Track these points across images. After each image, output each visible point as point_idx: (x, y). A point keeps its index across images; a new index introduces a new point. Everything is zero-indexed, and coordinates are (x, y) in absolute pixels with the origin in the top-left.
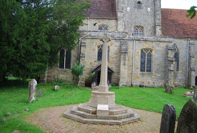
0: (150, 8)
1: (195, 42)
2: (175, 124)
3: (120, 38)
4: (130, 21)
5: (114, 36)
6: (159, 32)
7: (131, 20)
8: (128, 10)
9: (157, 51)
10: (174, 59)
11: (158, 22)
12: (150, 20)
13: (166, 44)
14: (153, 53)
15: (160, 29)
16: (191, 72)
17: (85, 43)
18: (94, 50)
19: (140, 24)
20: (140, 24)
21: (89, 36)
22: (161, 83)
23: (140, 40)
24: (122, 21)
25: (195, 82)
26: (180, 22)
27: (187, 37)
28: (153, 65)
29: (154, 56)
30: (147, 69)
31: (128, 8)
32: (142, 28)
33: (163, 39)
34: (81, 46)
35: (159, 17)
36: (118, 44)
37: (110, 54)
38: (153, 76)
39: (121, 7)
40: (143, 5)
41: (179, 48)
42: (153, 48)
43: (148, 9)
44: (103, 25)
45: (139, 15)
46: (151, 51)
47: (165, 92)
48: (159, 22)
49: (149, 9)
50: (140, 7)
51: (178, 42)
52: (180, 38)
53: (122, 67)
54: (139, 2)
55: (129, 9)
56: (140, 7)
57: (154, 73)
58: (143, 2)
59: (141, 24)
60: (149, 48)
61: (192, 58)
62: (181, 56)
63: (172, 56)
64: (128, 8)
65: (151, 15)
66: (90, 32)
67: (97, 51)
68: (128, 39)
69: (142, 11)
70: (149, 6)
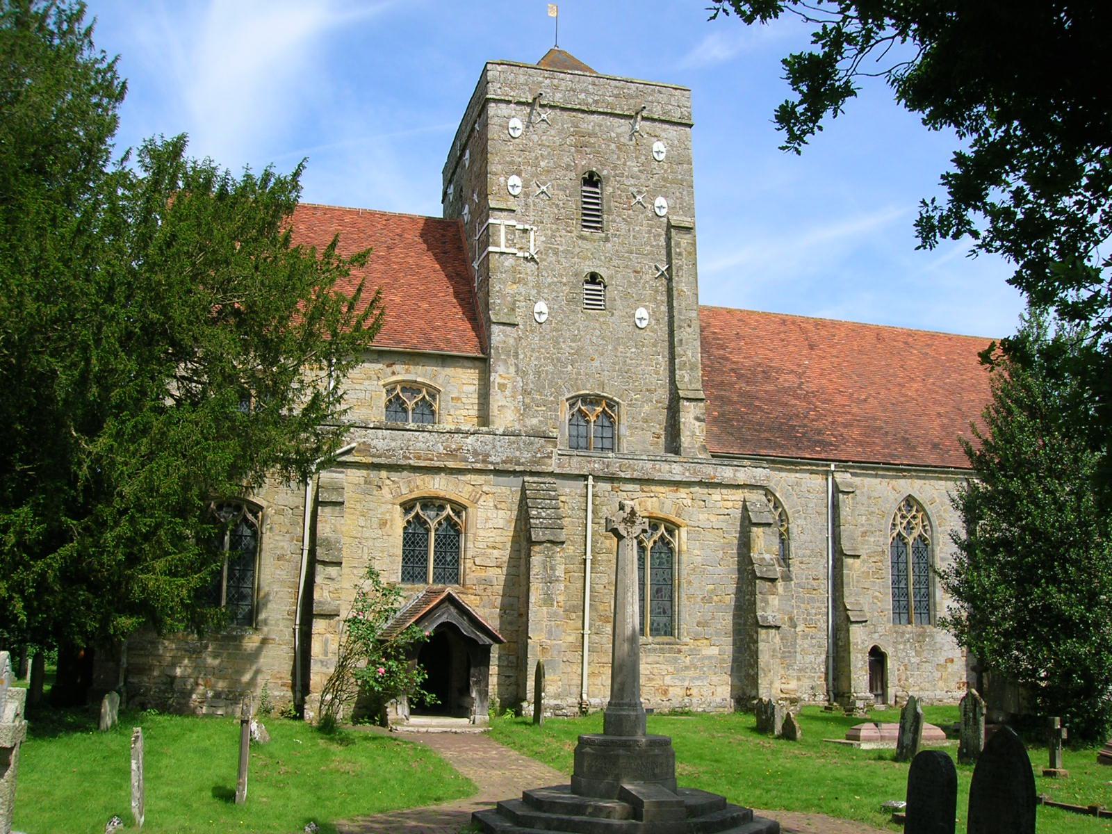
0: (646, 307)
1: (857, 480)
2: (1009, 732)
3: (518, 464)
4: (550, 368)
5: (488, 455)
6: (693, 434)
7: (555, 365)
8: (540, 313)
9: (696, 531)
10: (778, 569)
11: (686, 379)
12: (654, 372)
13: (738, 495)
14: (682, 540)
15: (697, 419)
16: (848, 631)
17: (339, 489)
18: (383, 524)
19: (602, 385)
20: (602, 385)
21: (359, 451)
22: (719, 689)
23: (619, 479)
24: (512, 370)
25: (867, 678)
26: (785, 381)
27: (823, 456)
28: (684, 601)
29: (684, 558)
30: (652, 624)
31: (541, 306)
32: (611, 407)
33: (727, 473)
34: (317, 503)
35: (690, 351)
36: (508, 490)
37: (470, 545)
38: (681, 656)
39: (504, 297)
40: (611, 292)
41: (789, 512)
42: (678, 515)
43: (637, 315)
44: (411, 388)
45: (592, 343)
46: (671, 533)
47: (753, 730)
48: (689, 381)
49: (641, 312)
50: (595, 302)
51: (781, 480)
52: (792, 464)
53: (538, 613)
54: (593, 278)
55: (545, 309)
56: (595, 302)
57: (686, 639)
58: (611, 277)
59: (607, 389)
60: (661, 515)
61: (850, 561)
62: (800, 552)
63: (767, 556)
64: (541, 306)
65: (654, 345)
66: (363, 432)
67: (401, 532)
68: (557, 471)
69: (610, 320)
70: (640, 301)
